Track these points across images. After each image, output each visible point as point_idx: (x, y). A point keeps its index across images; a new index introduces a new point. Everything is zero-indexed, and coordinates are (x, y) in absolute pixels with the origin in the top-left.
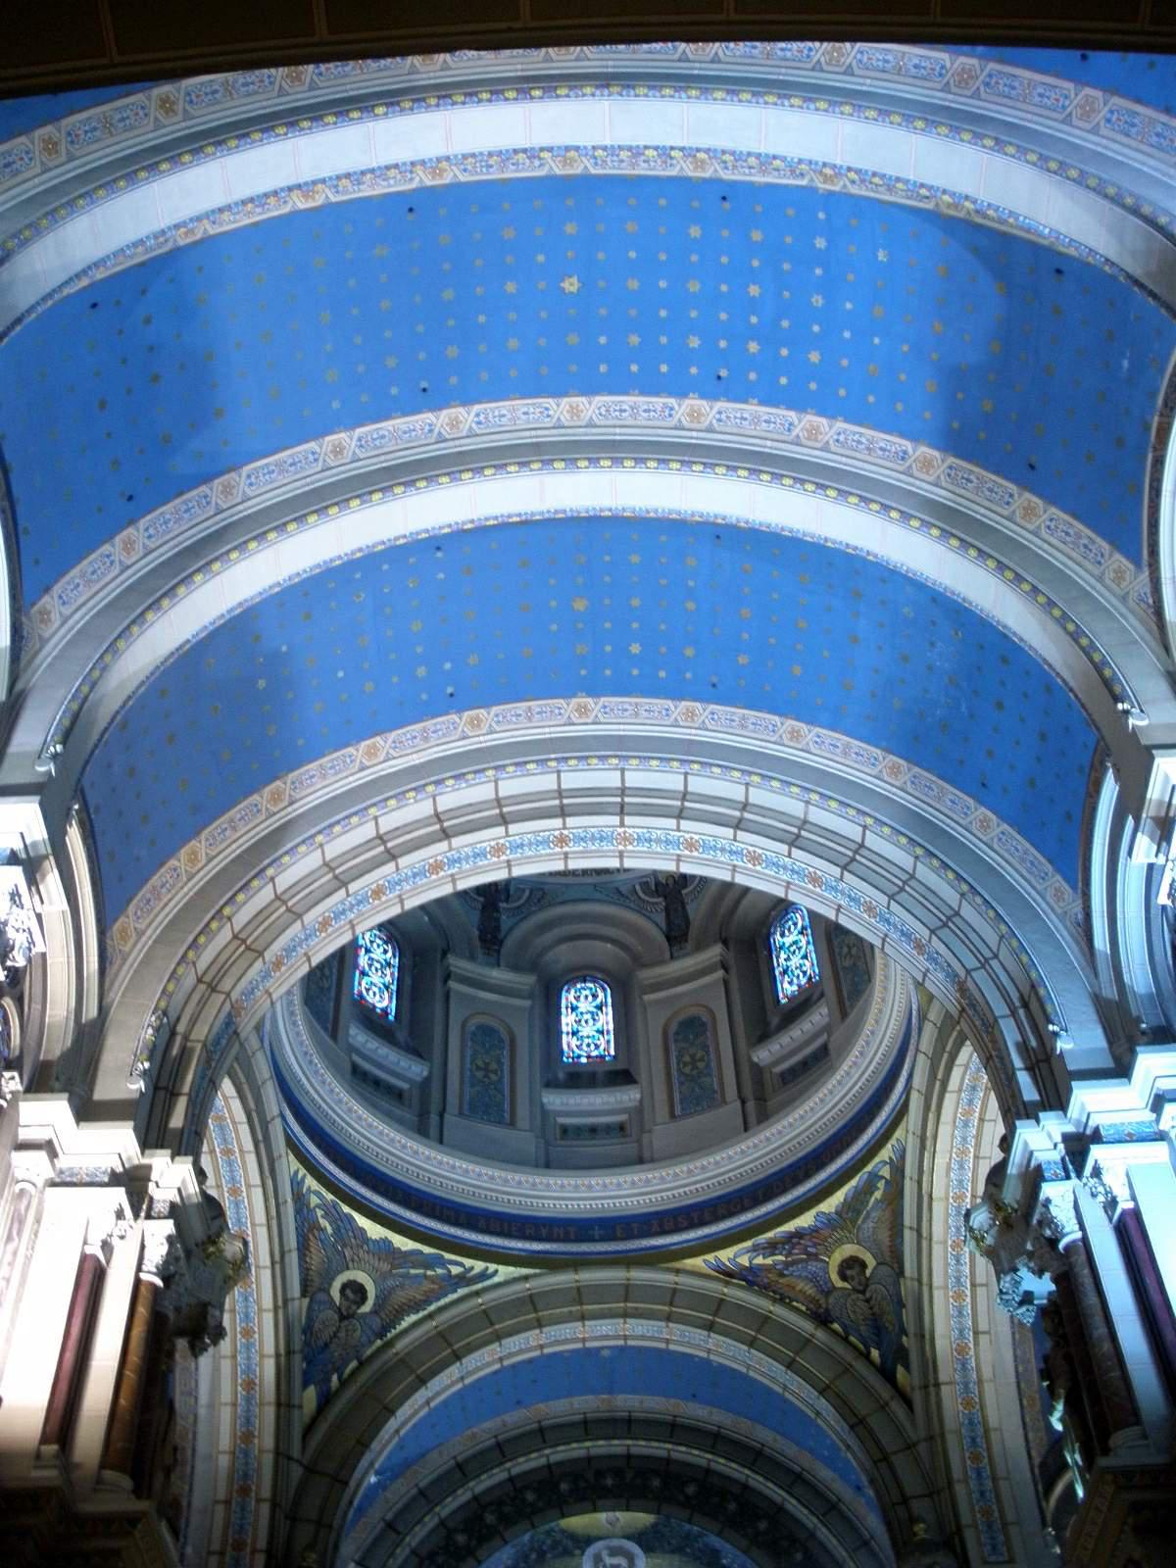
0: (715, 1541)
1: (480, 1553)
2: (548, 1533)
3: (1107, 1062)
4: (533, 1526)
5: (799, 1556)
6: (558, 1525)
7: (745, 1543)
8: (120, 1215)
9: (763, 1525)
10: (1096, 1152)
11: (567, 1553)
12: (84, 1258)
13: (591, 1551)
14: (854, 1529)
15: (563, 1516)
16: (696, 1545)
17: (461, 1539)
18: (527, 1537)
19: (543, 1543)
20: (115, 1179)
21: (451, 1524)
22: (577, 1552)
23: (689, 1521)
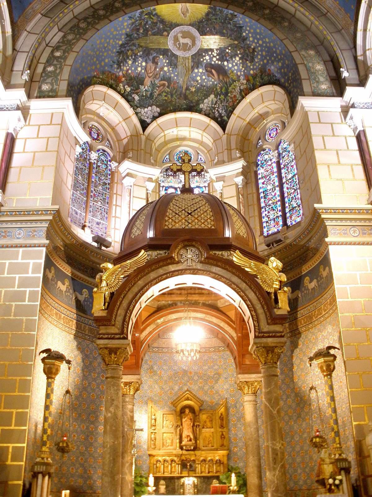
0: (242, 19)
1: (111, 18)
2: (149, 14)
3: (357, 82)
4: (142, 8)
5: (286, 24)
6: (154, 9)
7: (257, 17)
8: (19, 120)
9: (267, 11)
10: (352, 111)
11: (159, 33)
12: (8, 134)
13: (173, 33)
14: (319, 10)
15: (158, 4)
16: (229, 26)
17: (101, 12)
18: (137, 14)
19: (147, 22)
20: (18, 108)
21: (96, 7)
22: (165, 33)
23: (227, 8)
